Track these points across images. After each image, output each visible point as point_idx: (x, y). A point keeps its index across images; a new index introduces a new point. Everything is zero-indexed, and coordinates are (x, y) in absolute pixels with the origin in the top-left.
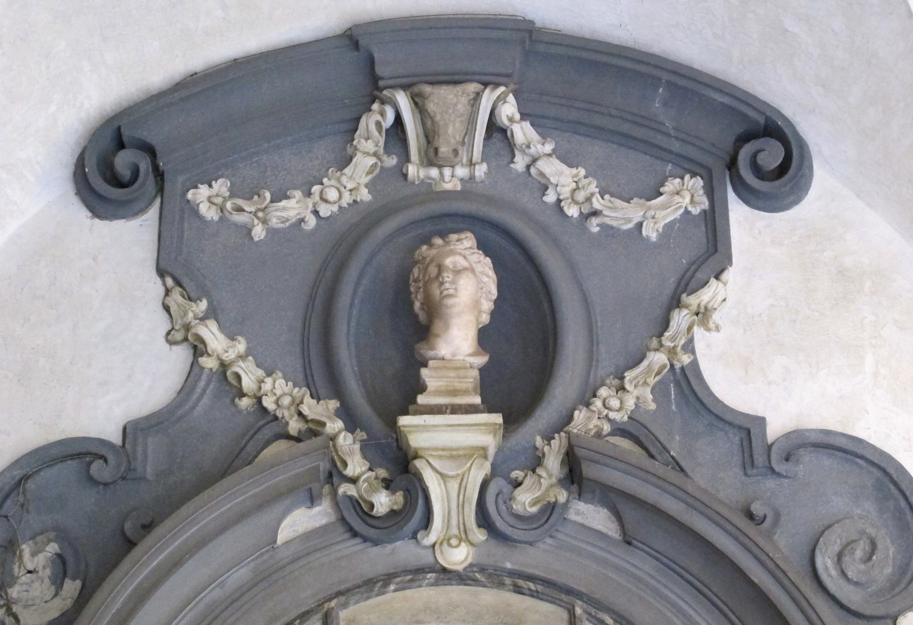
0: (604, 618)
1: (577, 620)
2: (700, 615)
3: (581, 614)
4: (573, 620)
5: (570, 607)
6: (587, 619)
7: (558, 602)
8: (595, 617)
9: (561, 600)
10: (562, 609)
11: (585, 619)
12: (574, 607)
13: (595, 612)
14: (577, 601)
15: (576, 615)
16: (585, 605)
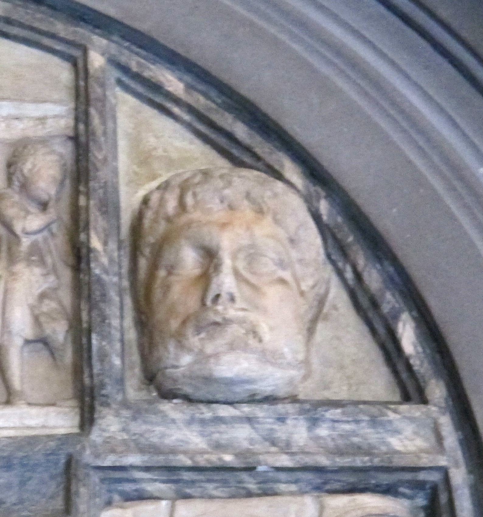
0: (162, 79)
1: (91, 81)
2: (407, 77)
3: (101, 67)
4: (82, 83)
5: (77, 53)
6: (119, 82)
7: (47, 41)
8: (137, 77)
9: (53, 36)
10: (55, 60)
11: (113, 81)
12: (85, 51)
13: (138, 63)
14: (95, 38)
15: (91, 71)
16: (113, 49)
